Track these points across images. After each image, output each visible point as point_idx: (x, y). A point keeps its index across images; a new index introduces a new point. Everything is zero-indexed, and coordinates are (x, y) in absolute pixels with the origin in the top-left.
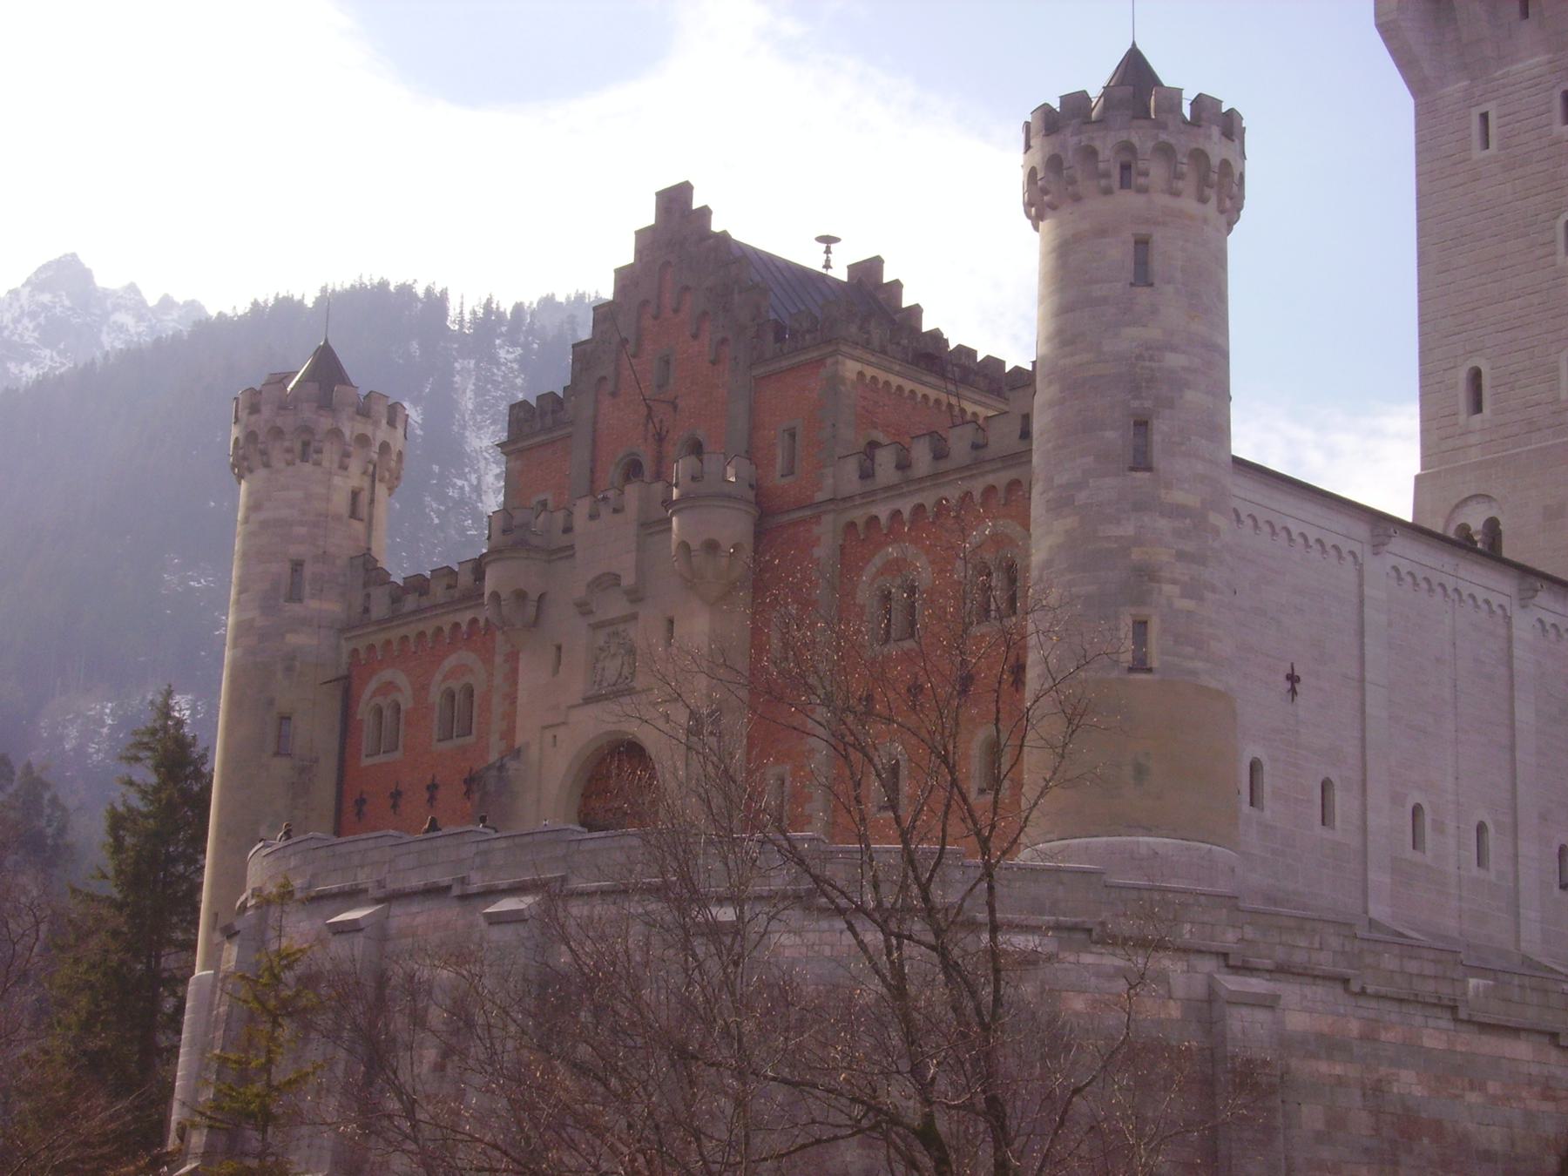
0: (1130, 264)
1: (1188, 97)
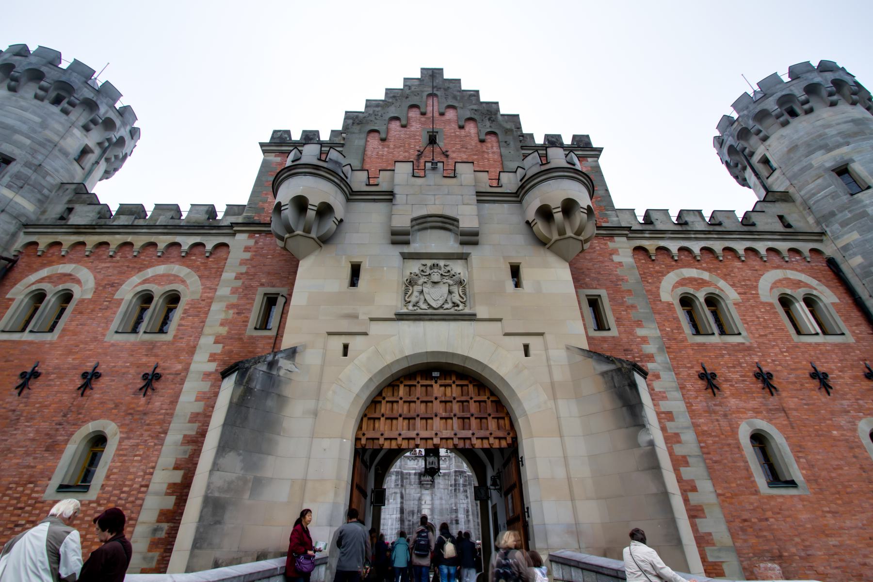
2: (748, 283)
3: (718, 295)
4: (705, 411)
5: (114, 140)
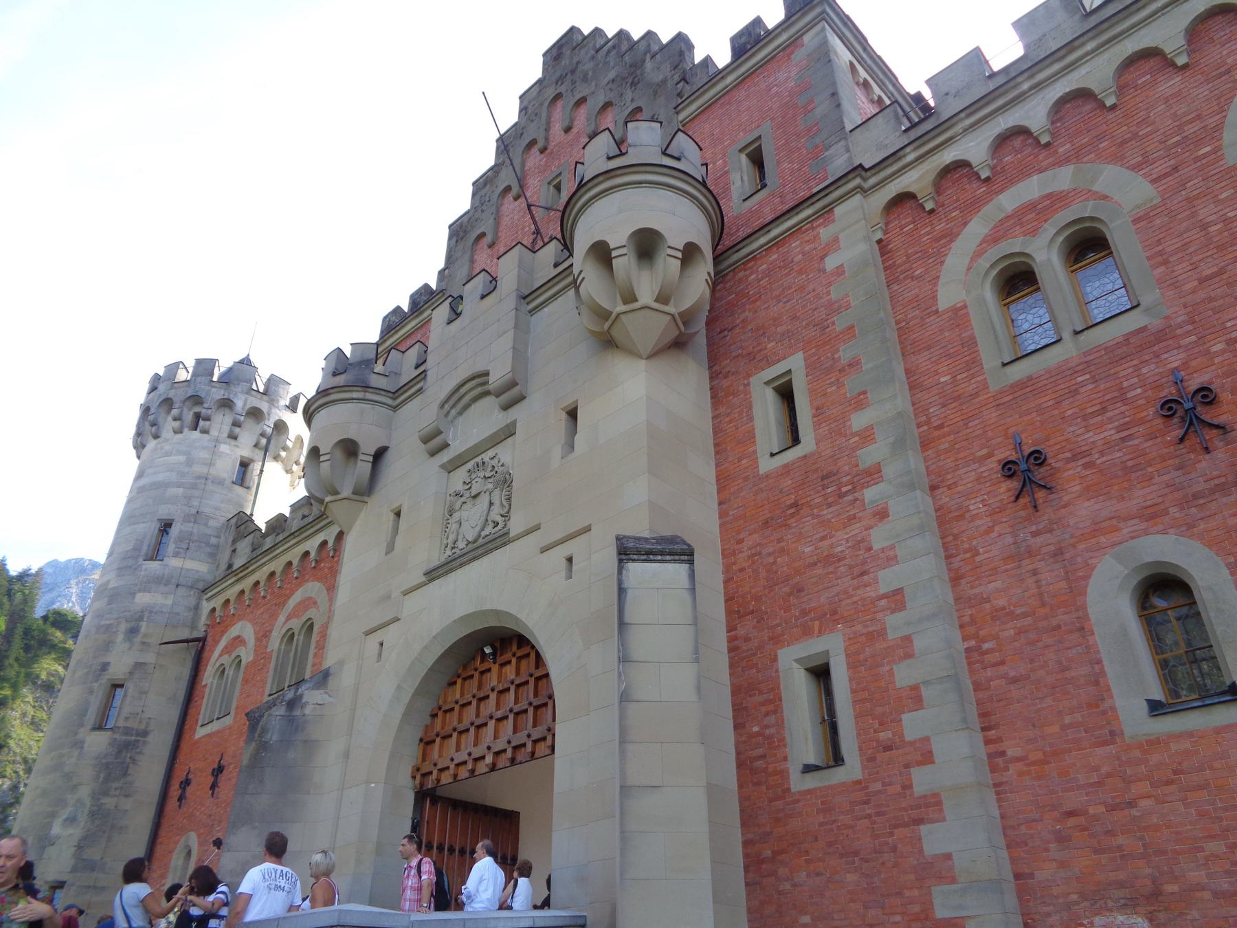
2: (1195, 127)
3: (1092, 219)
4: (1007, 559)
5: (269, 431)
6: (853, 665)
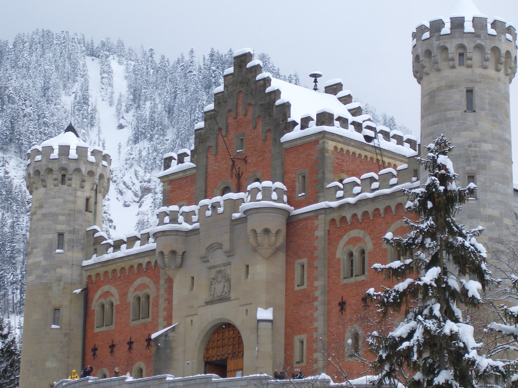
0: (464, 101)
1: (490, 21)
5: (97, 181)
6: (307, 342)
